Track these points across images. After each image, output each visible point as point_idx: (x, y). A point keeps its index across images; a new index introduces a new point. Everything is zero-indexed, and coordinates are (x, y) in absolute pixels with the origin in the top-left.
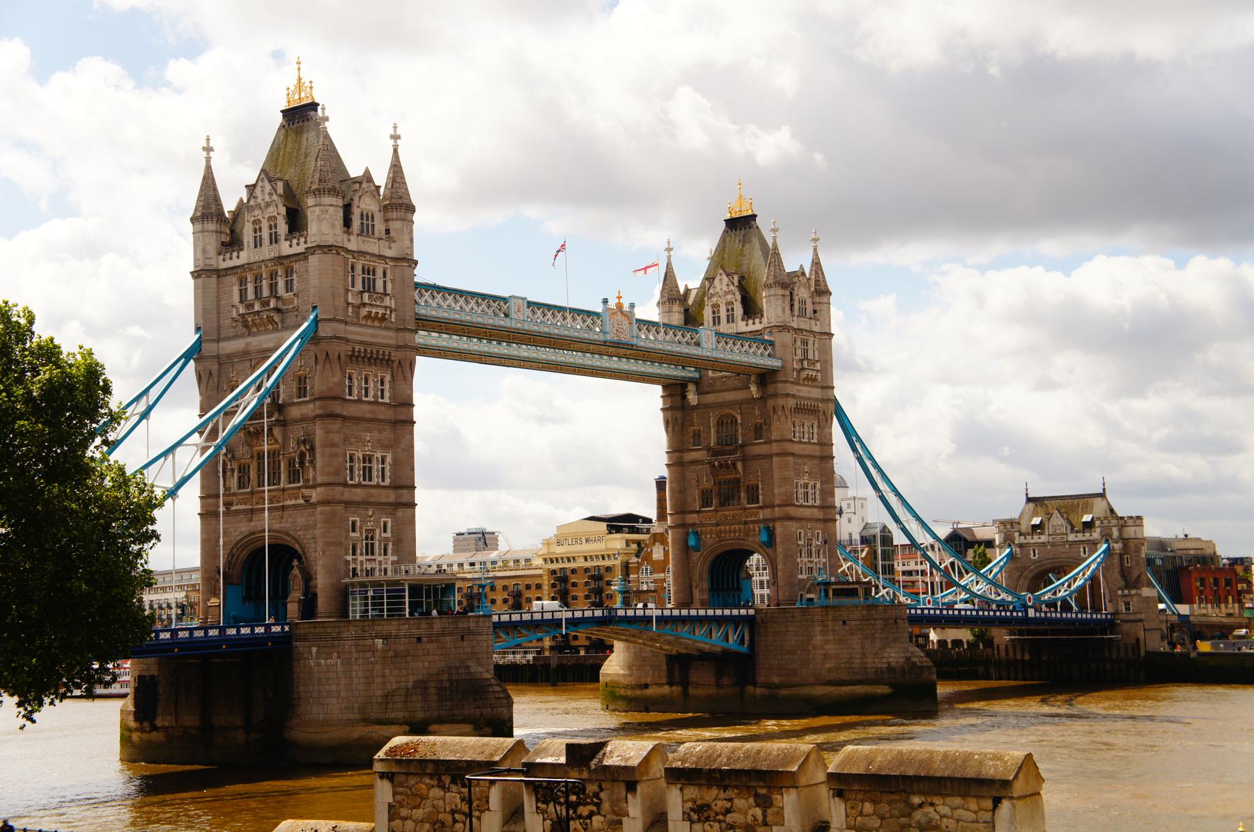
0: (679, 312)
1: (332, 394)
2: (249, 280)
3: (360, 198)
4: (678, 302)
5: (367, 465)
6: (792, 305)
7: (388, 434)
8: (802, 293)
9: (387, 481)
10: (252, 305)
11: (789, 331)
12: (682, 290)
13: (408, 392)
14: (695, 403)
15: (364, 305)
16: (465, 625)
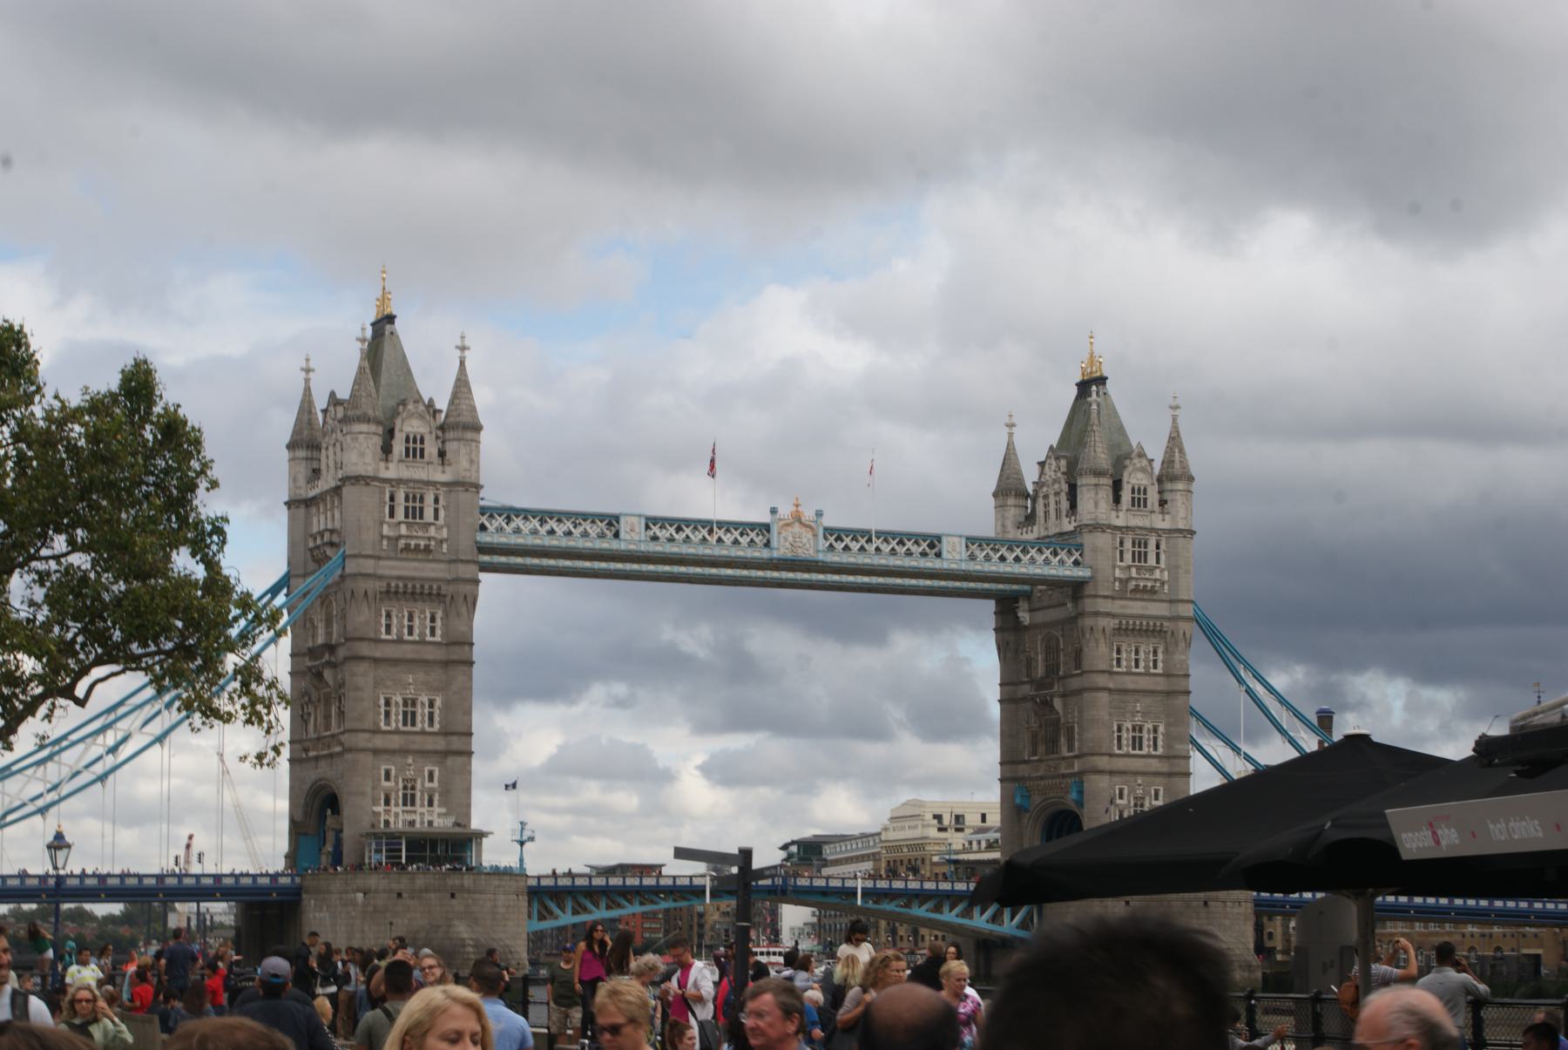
0: (1015, 506)
1: (357, 635)
2: (321, 510)
3: (403, 421)
4: (1013, 493)
5: (410, 709)
6: (1117, 500)
7: (436, 675)
8: (1133, 478)
9: (437, 727)
10: (315, 539)
11: (1104, 532)
12: (1030, 476)
13: (464, 628)
14: (1026, 623)
15: (400, 537)
16: (457, 882)
